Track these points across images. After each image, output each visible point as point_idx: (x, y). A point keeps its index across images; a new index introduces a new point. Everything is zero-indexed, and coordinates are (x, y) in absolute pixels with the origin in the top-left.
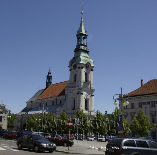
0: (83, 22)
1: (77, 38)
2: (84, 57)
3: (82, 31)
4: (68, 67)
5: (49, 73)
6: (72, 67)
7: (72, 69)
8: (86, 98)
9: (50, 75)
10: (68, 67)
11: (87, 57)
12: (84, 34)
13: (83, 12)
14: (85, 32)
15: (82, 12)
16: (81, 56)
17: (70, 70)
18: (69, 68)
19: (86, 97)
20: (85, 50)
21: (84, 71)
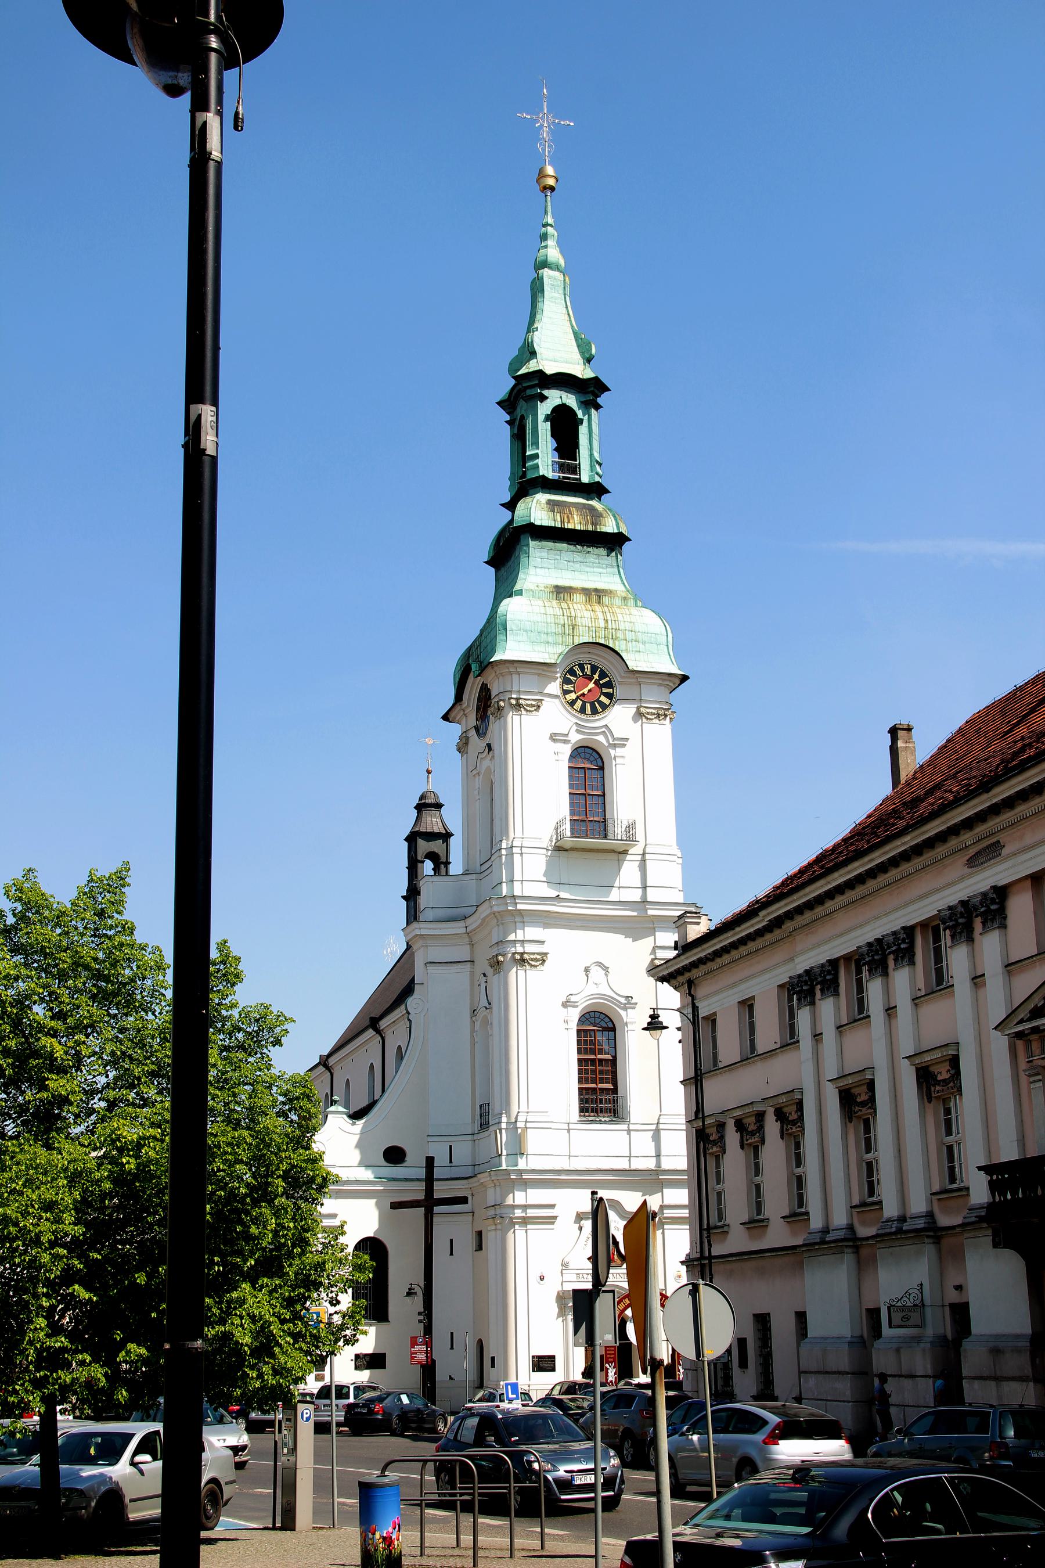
0: (556, 267)
1: (510, 423)
2: (561, 592)
3: (533, 354)
4: (446, 718)
5: (426, 805)
6: (472, 721)
7: (473, 732)
8: (592, 996)
9: (432, 823)
10: (446, 718)
11: (596, 595)
12: (564, 381)
13: (550, 170)
14: (582, 353)
15: (542, 175)
16: (520, 593)
17: (463, 746)
18: (455, 730)
19: (592, 989)
20: (576, 523)
21: (554, 738)
